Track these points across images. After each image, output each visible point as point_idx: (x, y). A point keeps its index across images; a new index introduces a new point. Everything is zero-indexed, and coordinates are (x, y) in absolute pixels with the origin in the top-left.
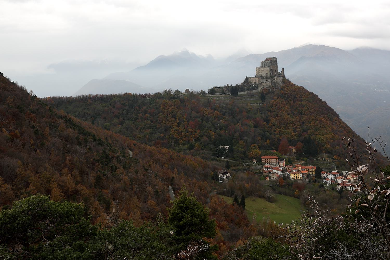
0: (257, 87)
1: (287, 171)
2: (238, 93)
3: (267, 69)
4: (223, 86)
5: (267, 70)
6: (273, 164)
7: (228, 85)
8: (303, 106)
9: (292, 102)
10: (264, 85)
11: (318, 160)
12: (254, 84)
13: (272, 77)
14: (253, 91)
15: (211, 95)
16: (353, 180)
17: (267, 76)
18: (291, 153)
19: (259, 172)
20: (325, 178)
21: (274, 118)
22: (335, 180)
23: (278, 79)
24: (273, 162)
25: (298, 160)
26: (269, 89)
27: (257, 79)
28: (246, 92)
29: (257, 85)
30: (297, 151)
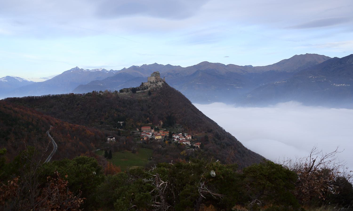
0: (148, 88)
1: (154, 135)
4: (129, 88)
6: (148, 131)
7: (131, 87)
11: (173, 128)
13: (156, 82)
14: (145, 90)
16: (188, 138)
18: (160, 124)
19: (138, 136)
20: (174, 138)
22: (179, 138)
24: (148, 130)
25: (163, 128)
27: (148, 83)
29: (147, 87)
30: (163, 123)
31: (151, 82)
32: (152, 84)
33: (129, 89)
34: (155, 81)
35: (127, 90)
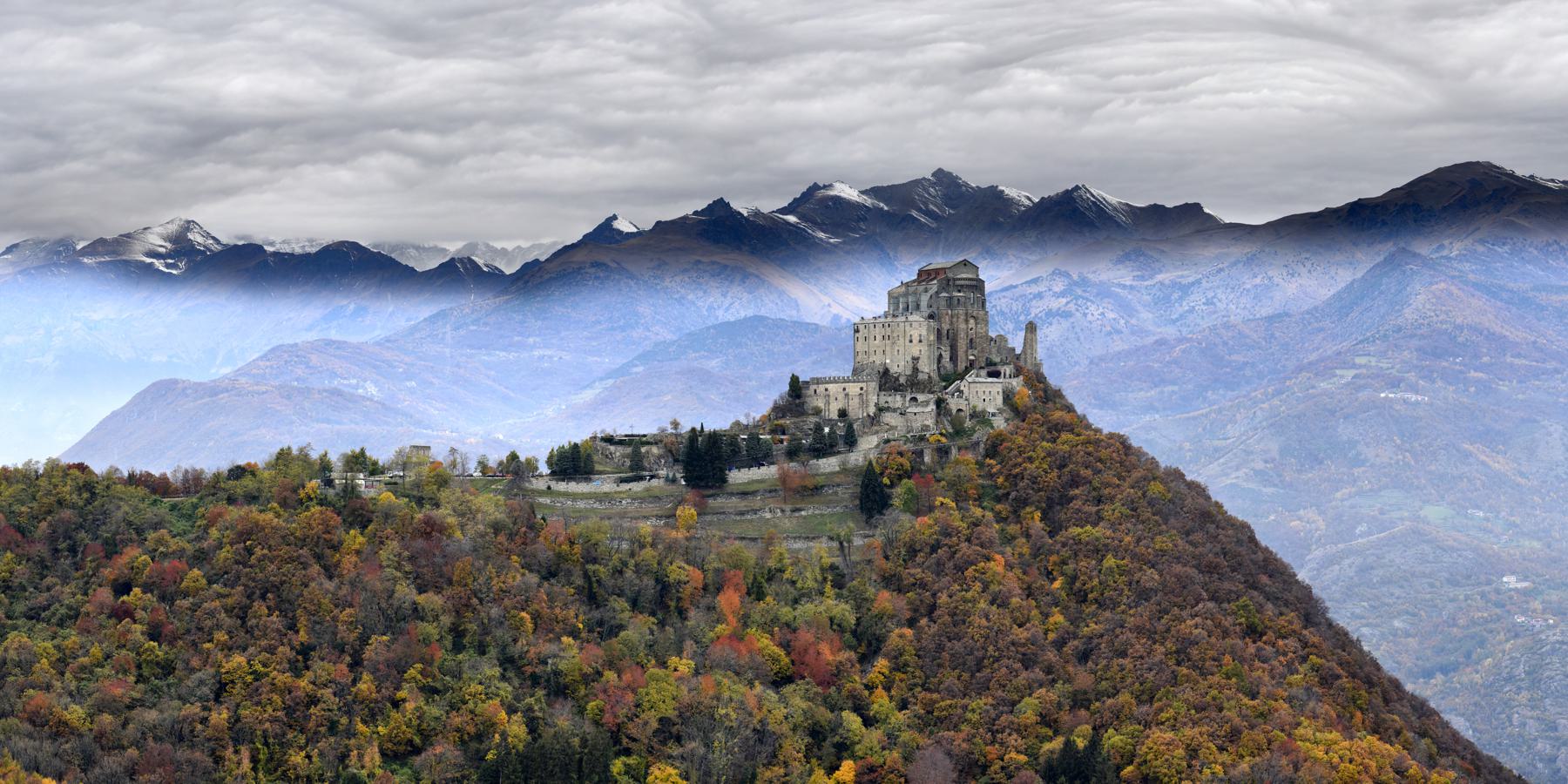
0: (851, 441)
2: (722, 471)
3: (918, 327)
5: (916, 339)
7: (676, 425)
8: (1098, 551)
9: (1036, 523)
10: (893, 428)
12: (830, 422)
13: (948, 379)
14: (822, 461)
15: (562, 486)
17: (916, 370)
21: (911, 623)
23: (980, 388)
26: (920, 454)
27: (854, 389)
28: (768, 472)
29: (850, 427)
31: (886, 371)
32: (897, 401)
33: (655, 441)
34: (927, 368)
35: (634, 455)
